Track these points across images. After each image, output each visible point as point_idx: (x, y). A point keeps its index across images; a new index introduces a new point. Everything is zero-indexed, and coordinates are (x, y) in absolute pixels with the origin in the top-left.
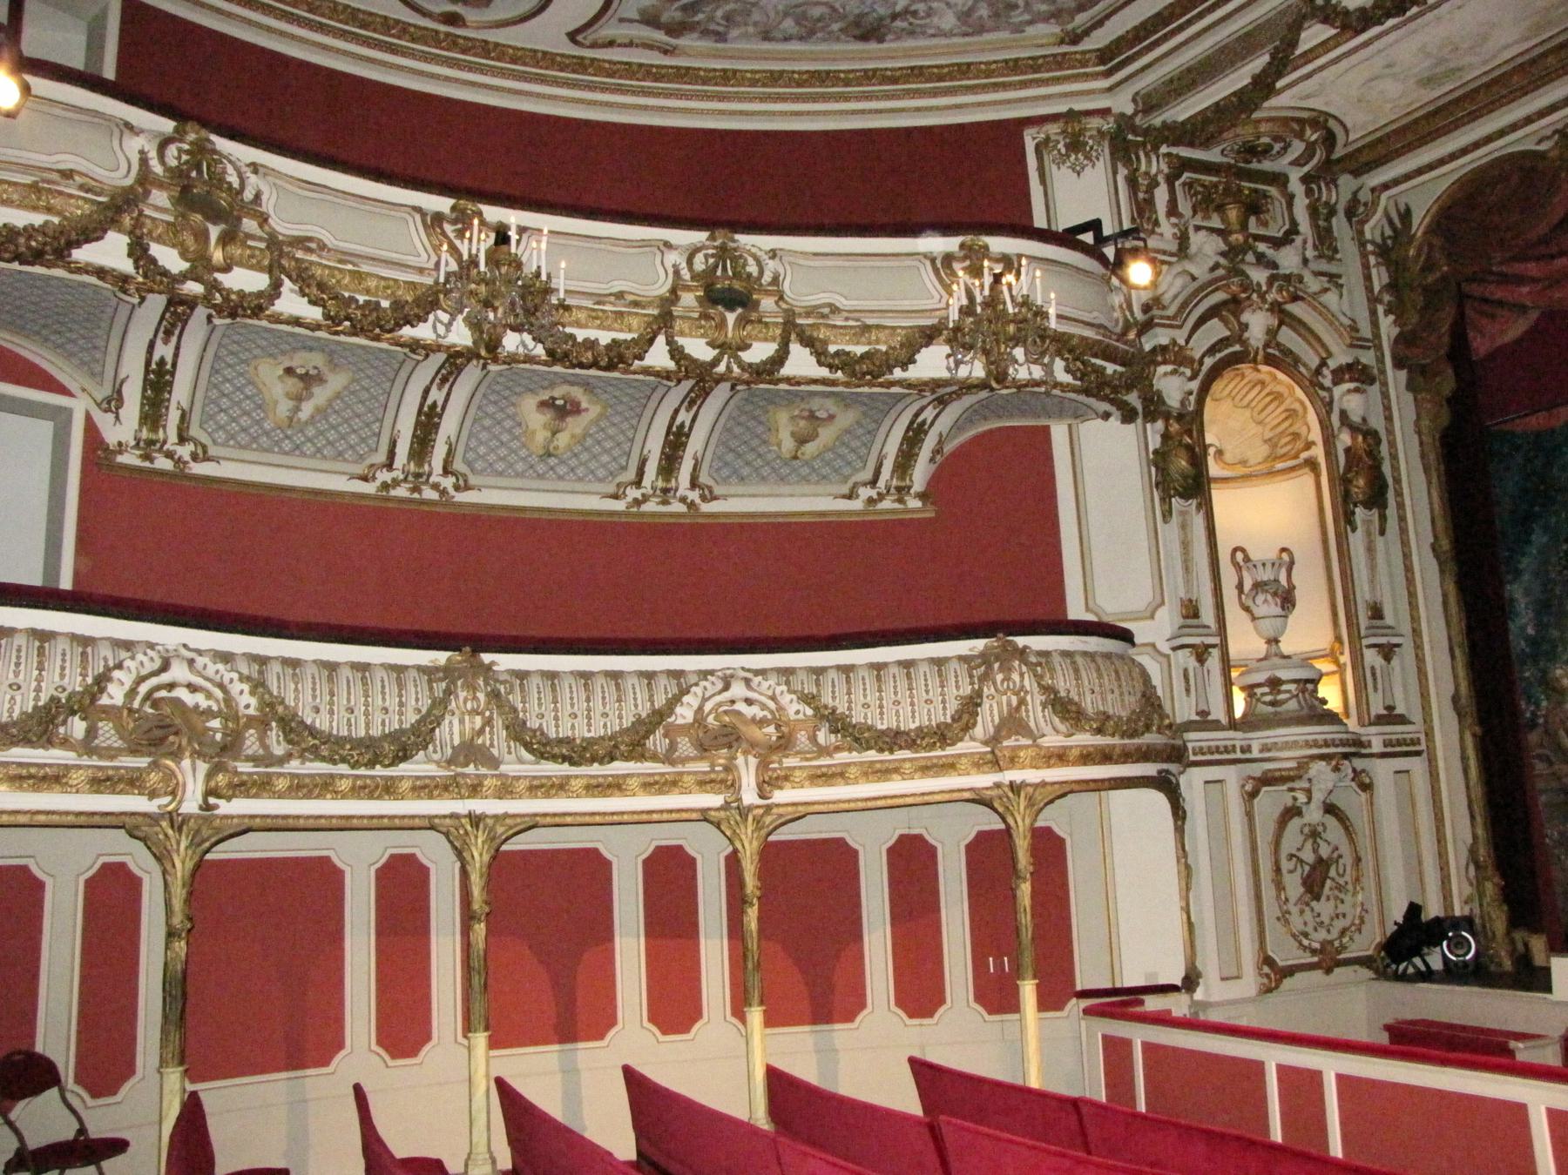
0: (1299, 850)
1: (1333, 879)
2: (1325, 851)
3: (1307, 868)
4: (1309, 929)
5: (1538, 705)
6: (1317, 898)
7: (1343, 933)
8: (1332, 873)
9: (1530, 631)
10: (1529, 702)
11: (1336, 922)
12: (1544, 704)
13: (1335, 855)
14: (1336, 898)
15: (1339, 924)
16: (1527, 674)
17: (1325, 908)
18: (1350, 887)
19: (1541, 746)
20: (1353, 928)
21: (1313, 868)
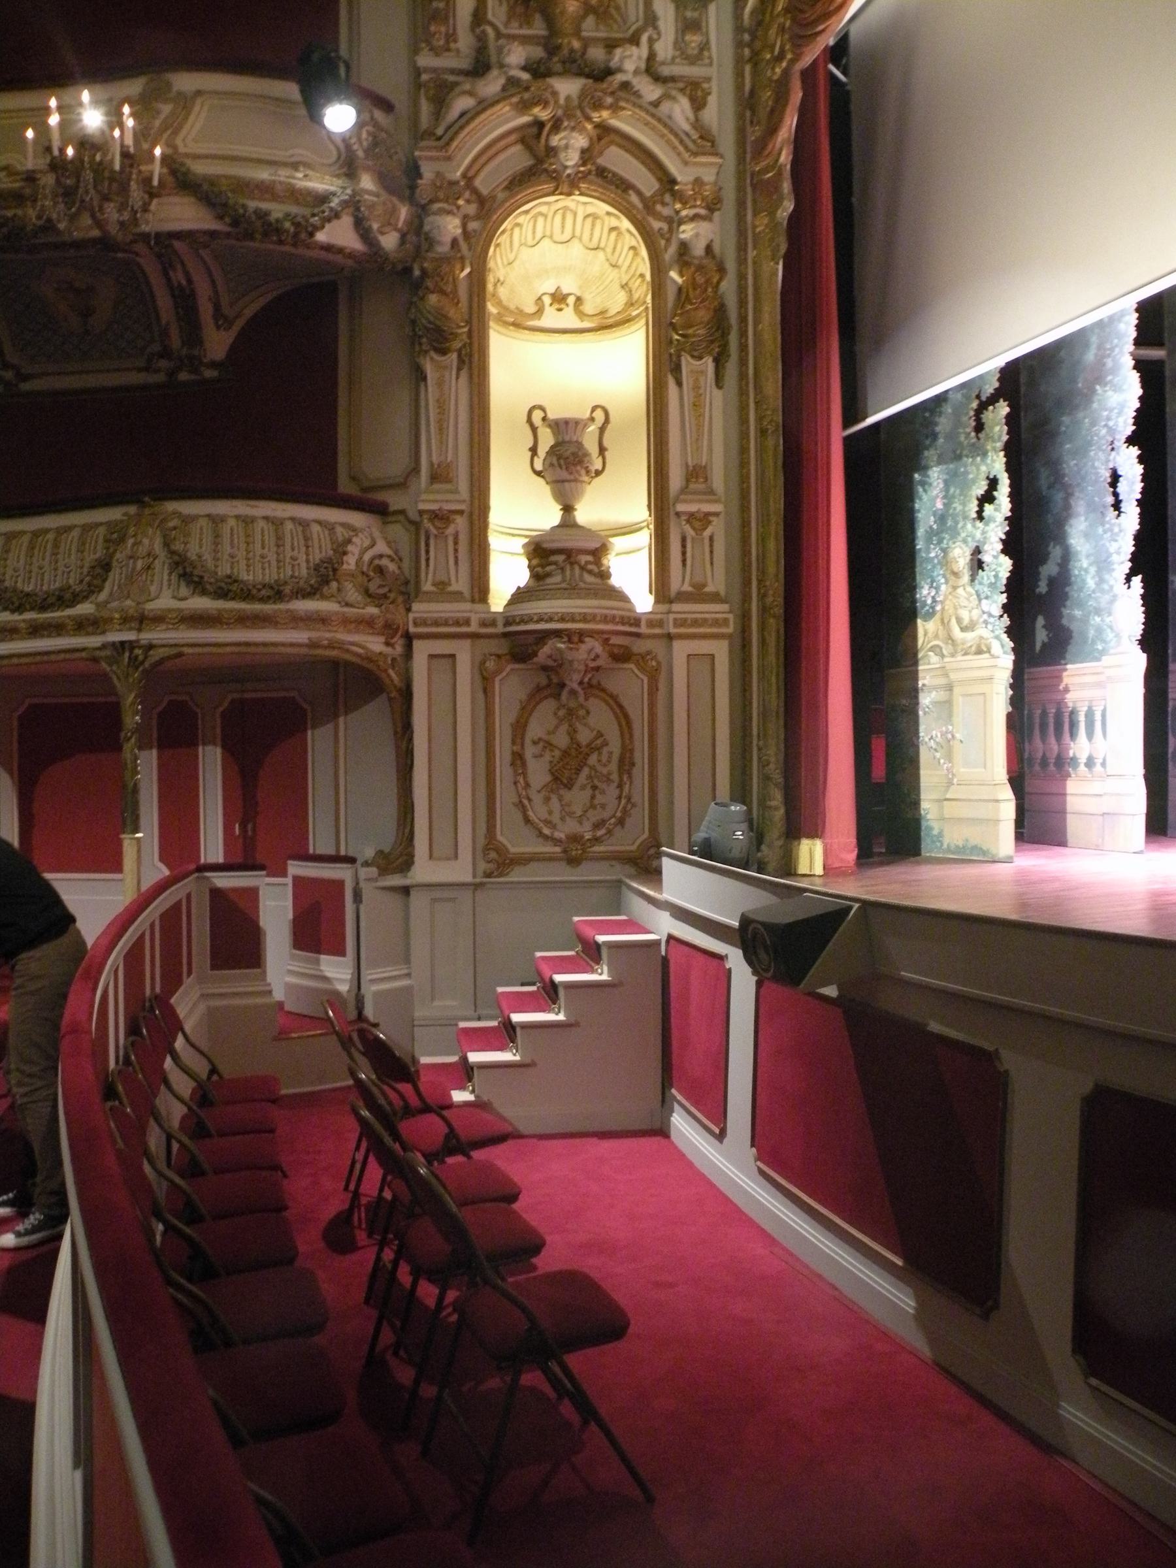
0: (549, 733)
1: (592, 768)
2: (584, 736)
3: (557, 753)
4: (556, 818)
5: (937, 589)
6: (569, 786)
7: (597, 826)
8: (593, 759)
9: (939, 505)
10: (931, 587)
11: (591, 813)
12: (943, 587)
13: (599, 742)
14: (595, 788)
15: (594, 816)
16: (932, 555)
17: (578, 797)
18: (615, 777)
19: (936, 637)
20: (613, 820)
21: (565, 753)
